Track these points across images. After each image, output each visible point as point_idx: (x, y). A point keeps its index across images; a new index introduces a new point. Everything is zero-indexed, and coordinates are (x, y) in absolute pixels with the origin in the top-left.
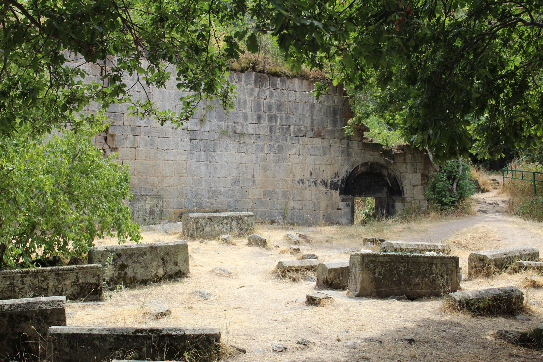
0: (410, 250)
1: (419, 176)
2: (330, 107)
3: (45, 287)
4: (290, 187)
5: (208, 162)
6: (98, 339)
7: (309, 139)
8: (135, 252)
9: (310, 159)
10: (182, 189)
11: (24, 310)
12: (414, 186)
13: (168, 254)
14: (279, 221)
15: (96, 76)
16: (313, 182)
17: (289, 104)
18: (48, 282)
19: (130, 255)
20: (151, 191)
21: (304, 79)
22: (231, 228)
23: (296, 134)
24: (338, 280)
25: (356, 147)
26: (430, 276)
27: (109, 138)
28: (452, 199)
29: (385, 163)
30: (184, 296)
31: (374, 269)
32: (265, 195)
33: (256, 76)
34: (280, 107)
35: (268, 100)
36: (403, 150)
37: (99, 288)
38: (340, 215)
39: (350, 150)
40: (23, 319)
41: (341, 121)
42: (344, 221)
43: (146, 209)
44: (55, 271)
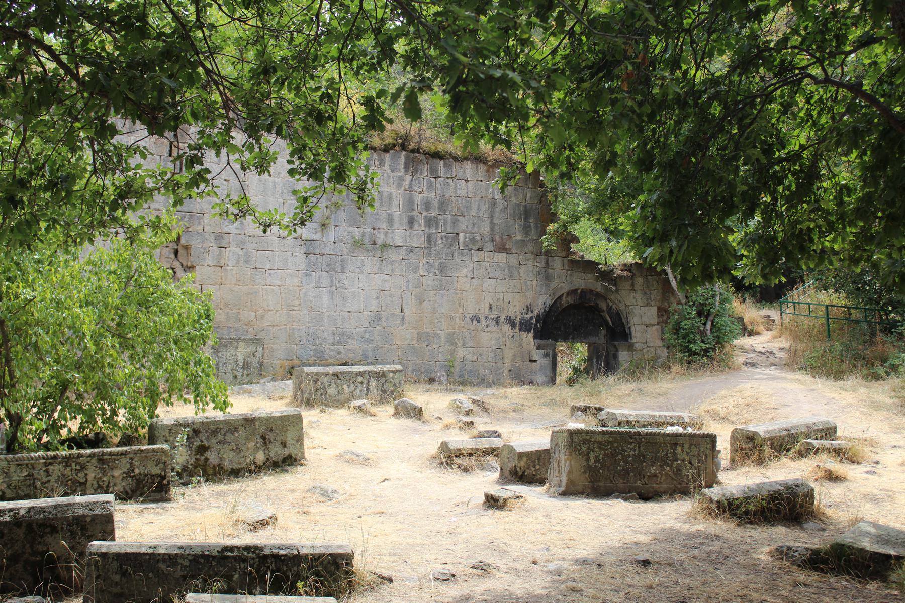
0: (642, 423)
1: (654, 310)
2: (519, 205)
3: (83, 481)
4: (459, 327)
5: (333, 288)
6: (164, 561)
7: (487, 254)
8: (221, 426)
9: (489, 284)
10: (293, 329)
11: (50, 516)
12: (647, 326)
13: (271, 430)
14: (442, 378)
15: (162, 157)
16: (493, 319)
17: (457, 201)
18: (86, 472)
19: (213, 431)
20: (245, 333)
21: (480, 162)
22: (368, 390)
23: (467, 246)
24: (533, 469)
25: (559, 267)
26: (672, 463)
27: (181, 252)
28: (704, 346)
29: (603, 291)
30: (297, 495)
31: (589, 453)
32: (419, 339)
33: (407, 158)
34: (443, 205)
35: (425, 195)
36: (630, 271)
37: (165, 482)
38: (534, 369)
39: (550, 271)
40: (48, 530)
41: (536, 227)
42: (540, 378)
43: (237, 361)
44: (98, 456)
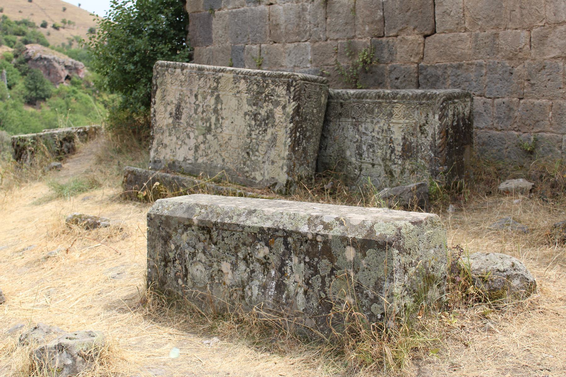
20: (506, 75)
22: (281, 287)
43: (391, 141)
